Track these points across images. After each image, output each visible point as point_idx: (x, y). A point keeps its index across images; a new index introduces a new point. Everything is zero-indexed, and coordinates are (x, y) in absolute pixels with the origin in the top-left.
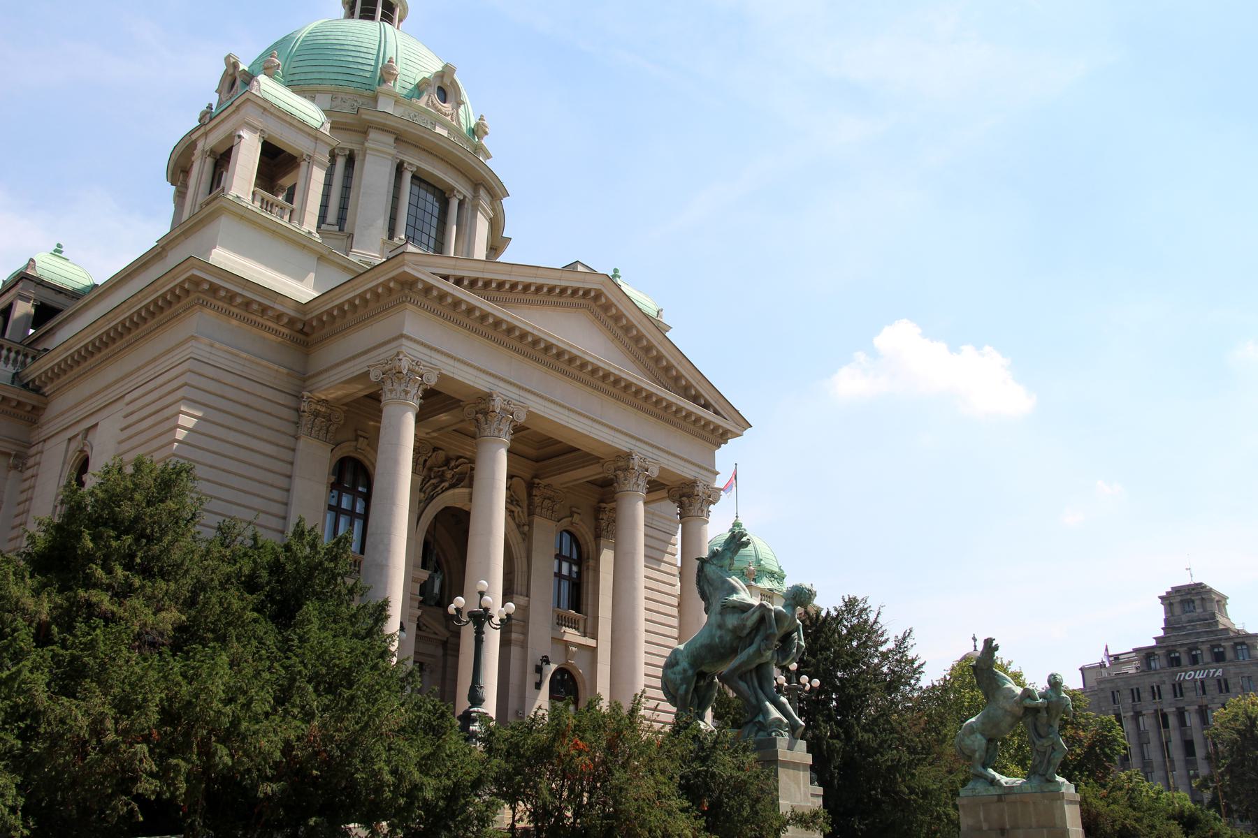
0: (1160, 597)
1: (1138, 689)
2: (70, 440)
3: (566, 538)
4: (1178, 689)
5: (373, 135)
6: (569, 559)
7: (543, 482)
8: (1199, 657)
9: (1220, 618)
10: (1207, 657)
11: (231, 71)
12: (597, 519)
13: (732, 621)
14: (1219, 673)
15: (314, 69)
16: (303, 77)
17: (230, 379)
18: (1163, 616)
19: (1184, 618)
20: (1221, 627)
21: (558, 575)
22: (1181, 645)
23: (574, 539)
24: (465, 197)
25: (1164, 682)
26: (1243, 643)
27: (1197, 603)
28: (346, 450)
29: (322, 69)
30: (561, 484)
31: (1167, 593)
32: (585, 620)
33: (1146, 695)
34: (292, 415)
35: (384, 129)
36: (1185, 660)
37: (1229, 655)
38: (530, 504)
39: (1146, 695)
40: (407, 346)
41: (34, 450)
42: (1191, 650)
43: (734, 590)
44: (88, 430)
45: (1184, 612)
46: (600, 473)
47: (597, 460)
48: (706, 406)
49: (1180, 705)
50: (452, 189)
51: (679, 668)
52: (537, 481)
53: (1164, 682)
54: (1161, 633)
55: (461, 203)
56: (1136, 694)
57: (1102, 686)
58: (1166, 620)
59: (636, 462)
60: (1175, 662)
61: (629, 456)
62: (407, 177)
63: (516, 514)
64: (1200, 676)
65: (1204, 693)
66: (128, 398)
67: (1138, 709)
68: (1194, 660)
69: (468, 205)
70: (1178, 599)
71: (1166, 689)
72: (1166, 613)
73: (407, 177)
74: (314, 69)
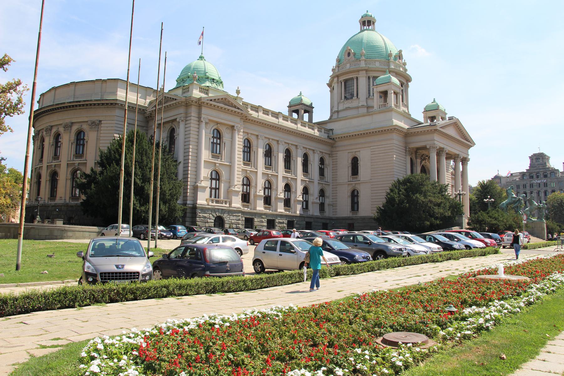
0: (529, 157)
1: (519, 185)
4: (532, 186)
8: (539, 176)
9: (547, 164)
10: (542, 176)
11: (348, 51)
13: (513, 199)
14: (545, 181)
15: (372, 54)
16: (370, 56)
17: (398, 146)
18: (529, 163)
19: (536, 164)
20: (547, 167)
22: (535, 172)
25: (527, 183)
26: (553, 172)
27: (541, 159)
29: (374, 53)
31: (532, 155)
33: (521, 187)
34: (404, 151)
35: (393, 72)
36: (535, 177)
37: (549, 175)
39: (521, 187)
42: (537, 174)
43: (513, 195)
45: (536, 162)
48: (469, 142)
49: (532, 190)
53: (527, 183)
54: (528, 168)
56: (518, 187)
57: (508, 184)
58: (530, 164)
59: (460, 156)
60: (532, 177)
61: (458, 155)
64: (539, 182)
65: (539, 187)
66: (372, 148)
67: (518, 191)
68: (538, 177)
70: (535, 157)
71: (528, 185)
72: (530, 162)
74: (372, 54)
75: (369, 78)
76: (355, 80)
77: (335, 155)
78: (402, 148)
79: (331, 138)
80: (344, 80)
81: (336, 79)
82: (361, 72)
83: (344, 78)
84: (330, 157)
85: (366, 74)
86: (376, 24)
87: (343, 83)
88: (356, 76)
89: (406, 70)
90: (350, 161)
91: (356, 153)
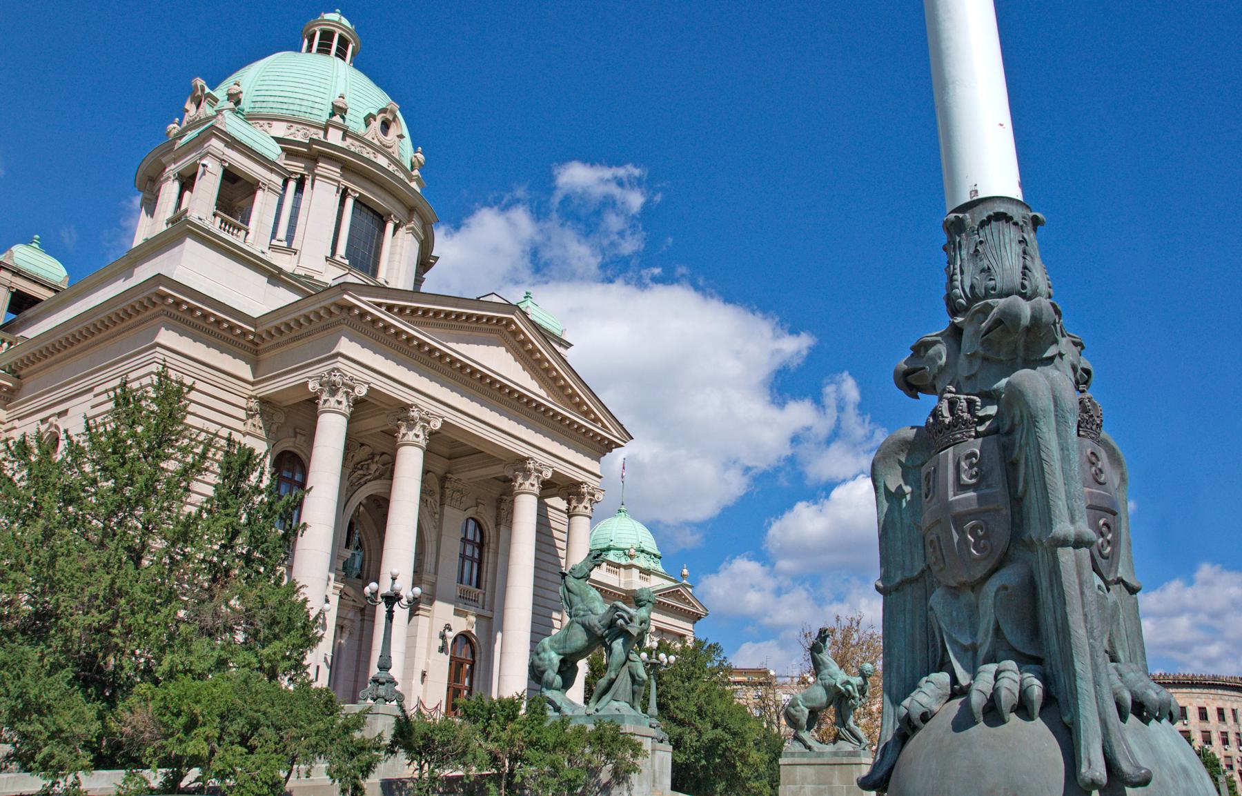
3: (471, 524)
6: (472, 542)
7: (455, 477)
12: (498, 508)
21: (463, 557)
23: (478, 525)
28: (287, 445)
30: (469, 479)
32: (484, 594)
35: (331, 159)
38: (442, 495)
40: (341, 363)
46: (500, 472)
47: (500, 461)
52: (449, 475)
62: (350, 202)
63: (429, 503)
66: (97, 390)
73: (350, 202)
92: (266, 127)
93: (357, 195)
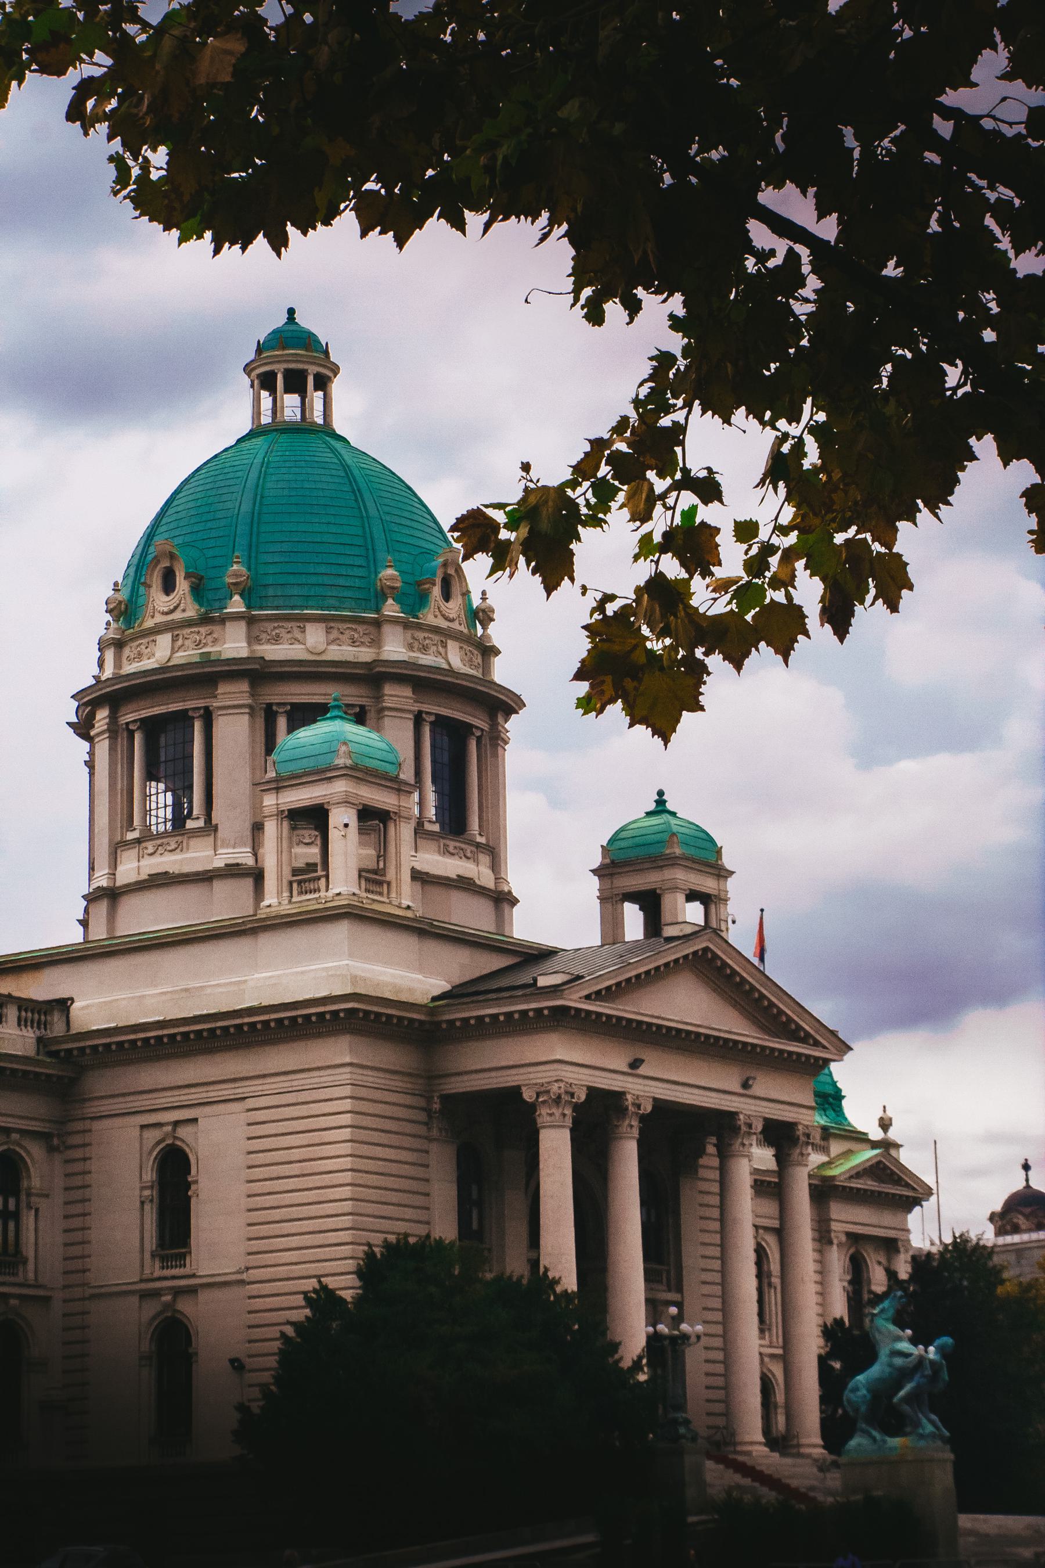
2: (143, 1127)
5: (388, 689)
24: (482, 730)
34: (422, 1116)
35: (400, 679)
41: (79, 1126)
44: (176, 1124)
48: (806, 1038)
50: (469, 728)
51: (859, 1393)
55: (479, 739)
66: (251, 1103)
69: (486, 741)
75: (270, 715)
76: (198, 726)
77: (77, 1140)
78: (408, 1100)
79: (54, 1048)
80: (143, 721)
81: (102, 715)
82: (222, 688)
83: (145, 713)
84: (51, 1149)
85: (252, 695)
86: (337, 387)
87: (138, 738)
88: (201, 703)
89: (489, 651)
90: (150, 1175)
91: (183, 1132)
92: (297, 634)
93: (432, 718)
